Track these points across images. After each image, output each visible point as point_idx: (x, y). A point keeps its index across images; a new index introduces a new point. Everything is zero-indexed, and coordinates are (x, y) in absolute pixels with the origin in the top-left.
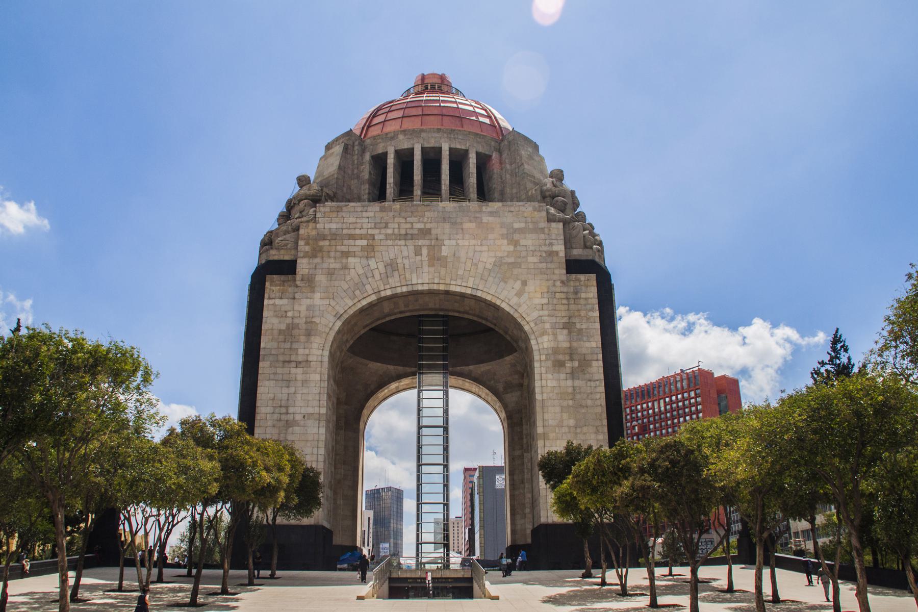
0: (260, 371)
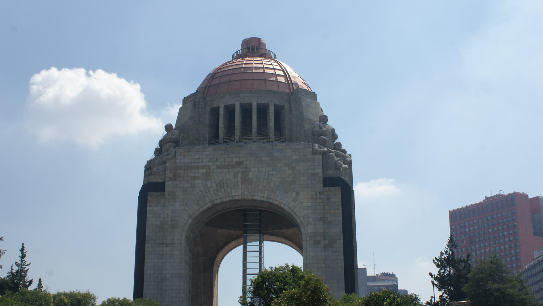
0: (146, 250)
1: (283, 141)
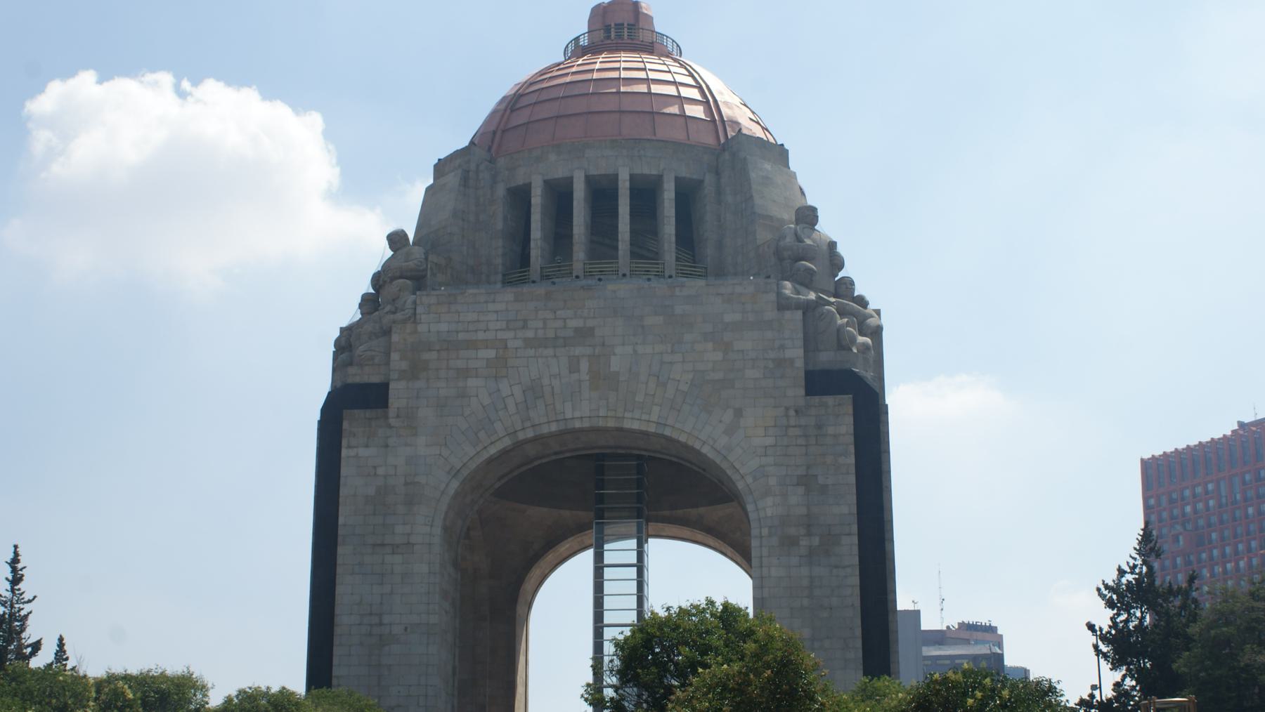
0: (340, 560)
1: (699, 276)
